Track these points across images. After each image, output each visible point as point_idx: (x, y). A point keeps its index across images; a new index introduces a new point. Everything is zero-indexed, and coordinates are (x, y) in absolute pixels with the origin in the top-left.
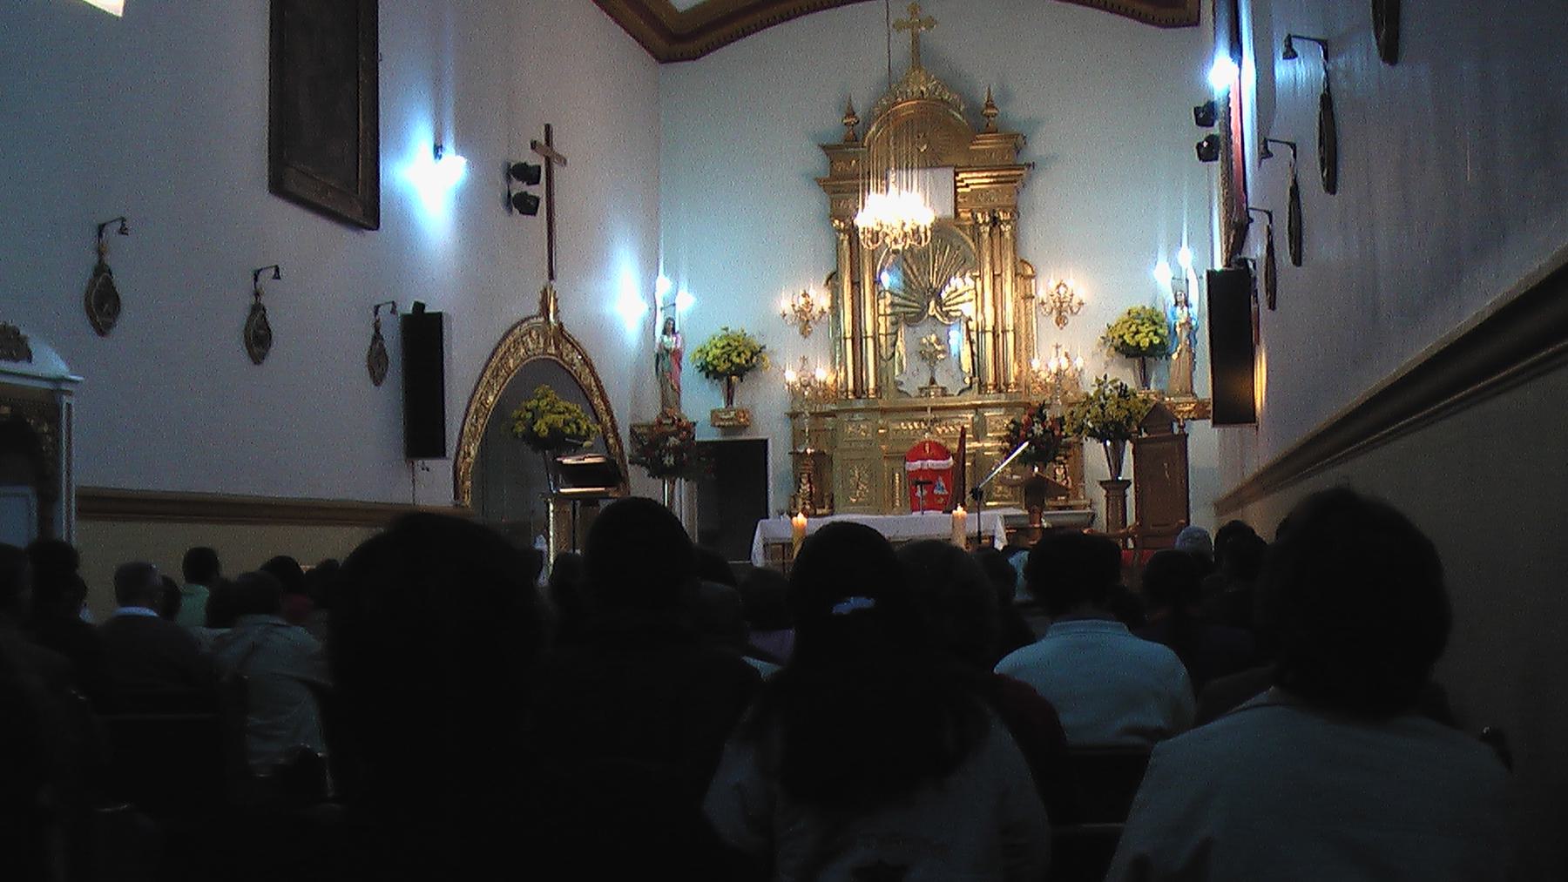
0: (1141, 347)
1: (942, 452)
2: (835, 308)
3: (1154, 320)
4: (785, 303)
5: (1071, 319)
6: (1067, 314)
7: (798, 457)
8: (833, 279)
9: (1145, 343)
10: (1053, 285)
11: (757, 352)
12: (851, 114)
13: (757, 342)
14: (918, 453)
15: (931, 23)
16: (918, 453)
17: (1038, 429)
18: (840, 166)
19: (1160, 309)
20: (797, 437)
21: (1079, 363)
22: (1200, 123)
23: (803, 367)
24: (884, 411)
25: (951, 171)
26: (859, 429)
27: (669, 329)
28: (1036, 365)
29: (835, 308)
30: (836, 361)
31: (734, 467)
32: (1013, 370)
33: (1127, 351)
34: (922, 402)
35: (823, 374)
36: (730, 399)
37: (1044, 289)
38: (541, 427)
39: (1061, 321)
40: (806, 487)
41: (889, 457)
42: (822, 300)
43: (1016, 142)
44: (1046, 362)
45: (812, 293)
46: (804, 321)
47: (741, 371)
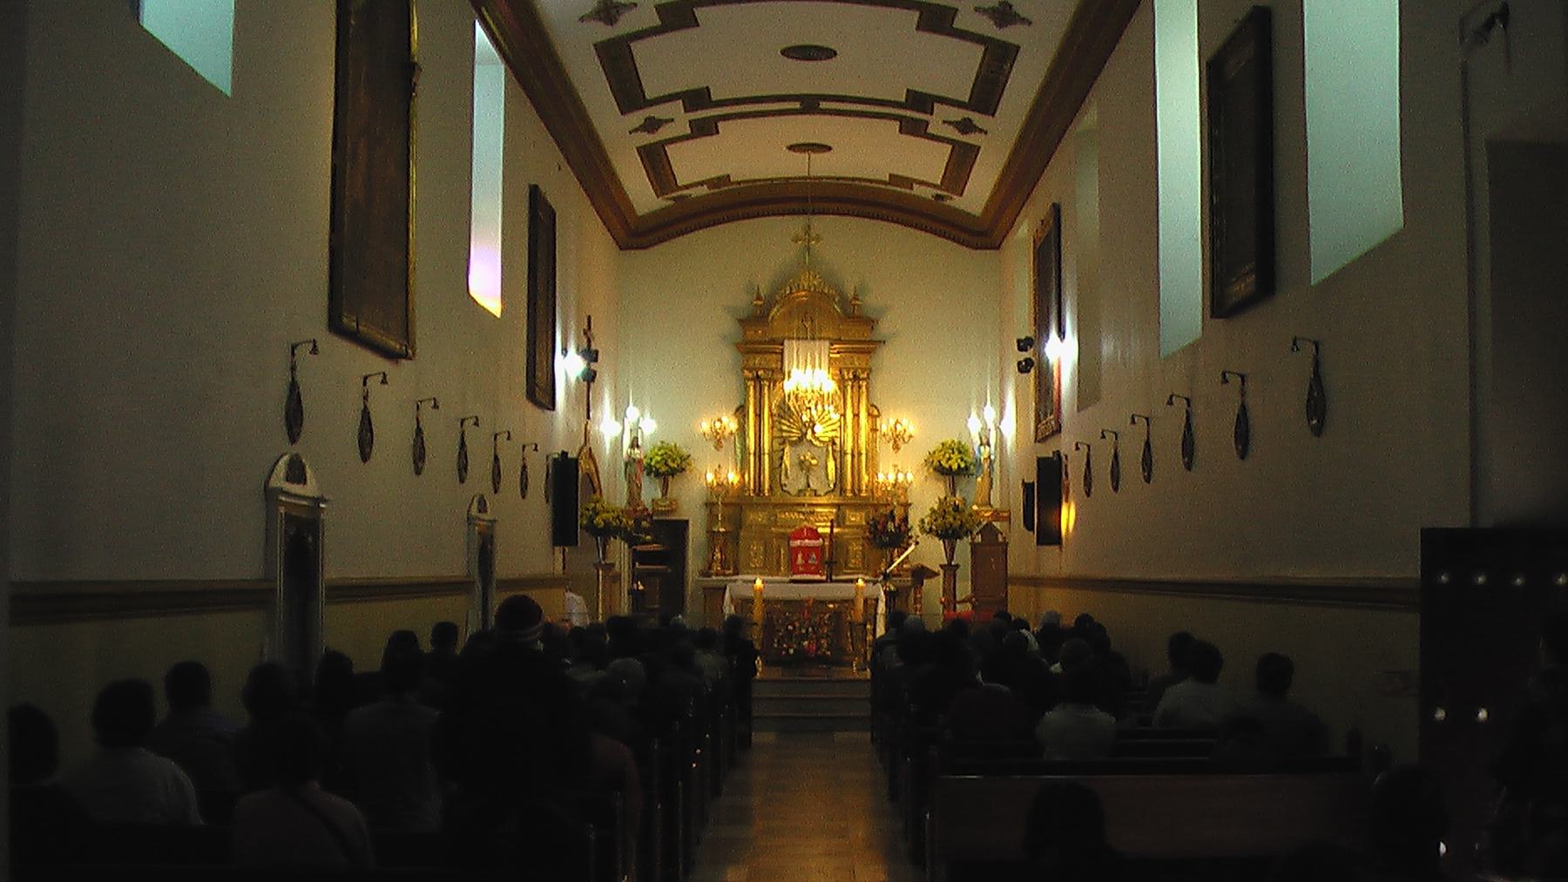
0: (952, 469)
1: (814, 534)
2: (742, 430)
3: (961, 450)
4: (705, 426)
5: (903, 447)
6: (900, 443)
7: (712, 534)
8: (741, 411)
9: (955, 467)
10: (892, 422)
11: (685, 459)
12: (759, 298)
13: (685, 452)
14: (798, 535)
15: (818, 239)
16: (798, 535)
17: (891, 526)
18: (750, 333)
19: (968, 445)
20: (712, 518)
21: (910, 477)
22: (1021, 349)
23: (717, 472)
24: (775, 506)
25: (827, 343)
26: (757, 517)
27: (634, 444)
28: (881, 478)
29: (742, 430)
30: (743, 471)
31: (661, 538)
32: (865, 478)
33: (942, 471)
34: (801, 500)
35: (733, 478)
36: (664, 494)
37: (885, 425)
38: (598, 520)
39: (896, 448)
40: (718, 555)
41: (782, 536)
42: (731, 424)
43: (870, 323)
44: (886, 475)
45: (725, 419)
46: (718, 440)
47: (673, 472)
